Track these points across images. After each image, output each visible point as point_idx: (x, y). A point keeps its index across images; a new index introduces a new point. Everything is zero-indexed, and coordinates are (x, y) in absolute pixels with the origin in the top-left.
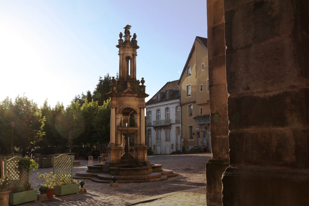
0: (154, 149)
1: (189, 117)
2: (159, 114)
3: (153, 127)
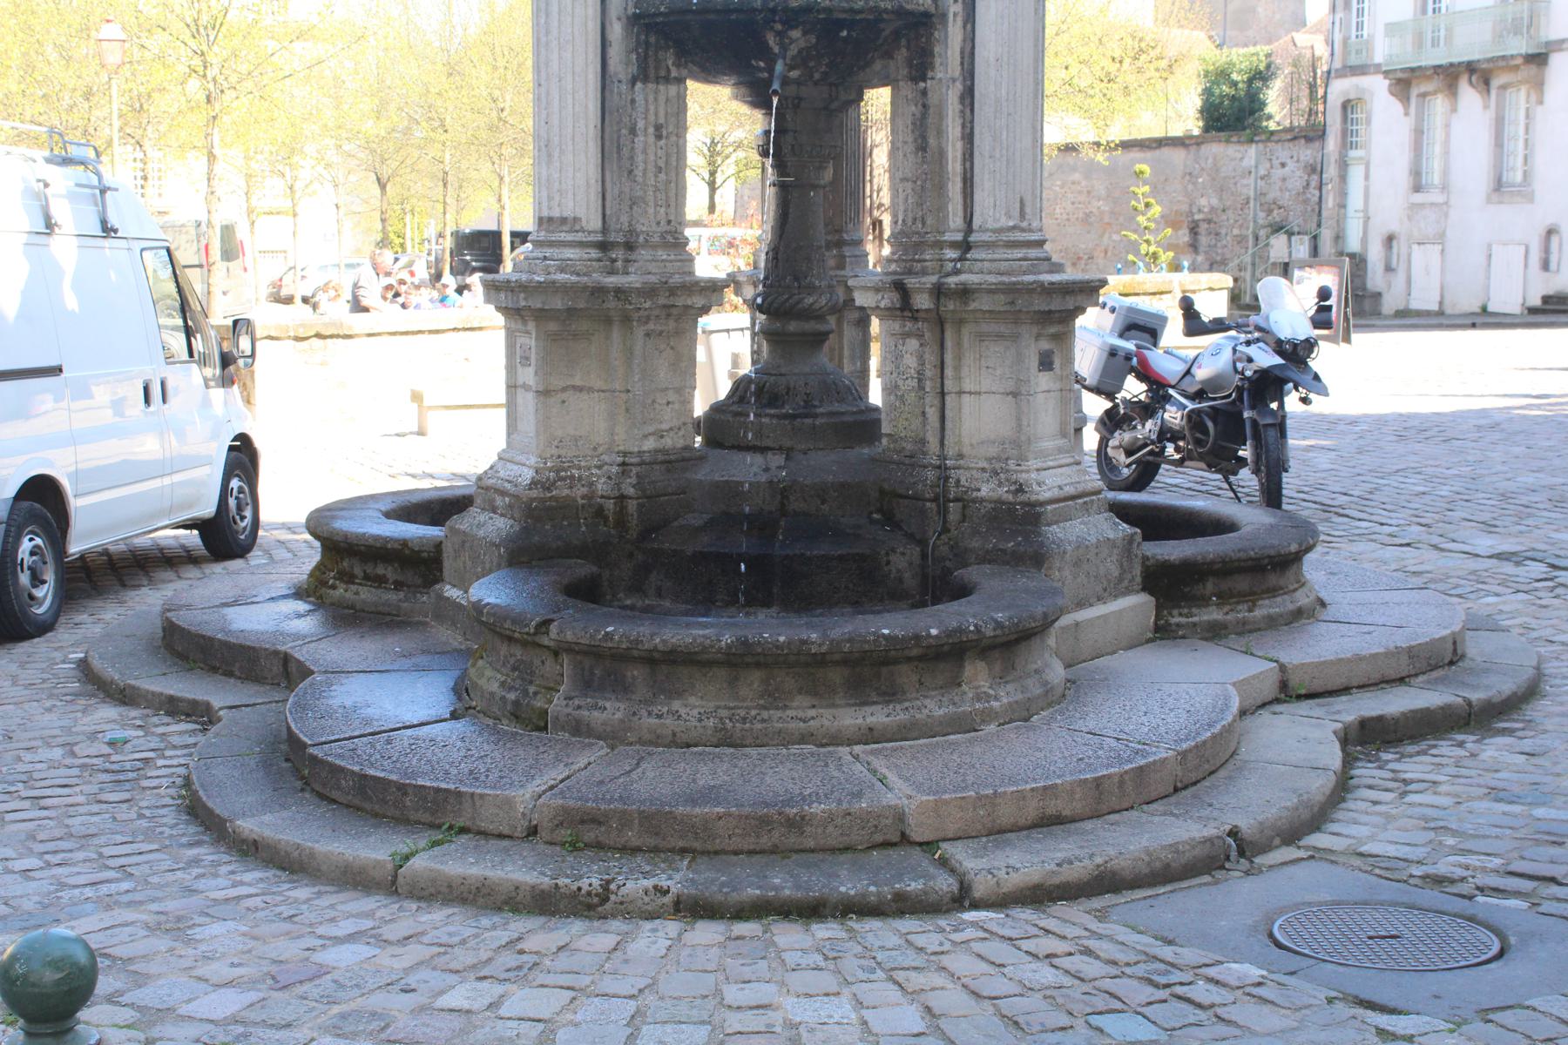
0: (1389, 269)
3: (1386, 73)
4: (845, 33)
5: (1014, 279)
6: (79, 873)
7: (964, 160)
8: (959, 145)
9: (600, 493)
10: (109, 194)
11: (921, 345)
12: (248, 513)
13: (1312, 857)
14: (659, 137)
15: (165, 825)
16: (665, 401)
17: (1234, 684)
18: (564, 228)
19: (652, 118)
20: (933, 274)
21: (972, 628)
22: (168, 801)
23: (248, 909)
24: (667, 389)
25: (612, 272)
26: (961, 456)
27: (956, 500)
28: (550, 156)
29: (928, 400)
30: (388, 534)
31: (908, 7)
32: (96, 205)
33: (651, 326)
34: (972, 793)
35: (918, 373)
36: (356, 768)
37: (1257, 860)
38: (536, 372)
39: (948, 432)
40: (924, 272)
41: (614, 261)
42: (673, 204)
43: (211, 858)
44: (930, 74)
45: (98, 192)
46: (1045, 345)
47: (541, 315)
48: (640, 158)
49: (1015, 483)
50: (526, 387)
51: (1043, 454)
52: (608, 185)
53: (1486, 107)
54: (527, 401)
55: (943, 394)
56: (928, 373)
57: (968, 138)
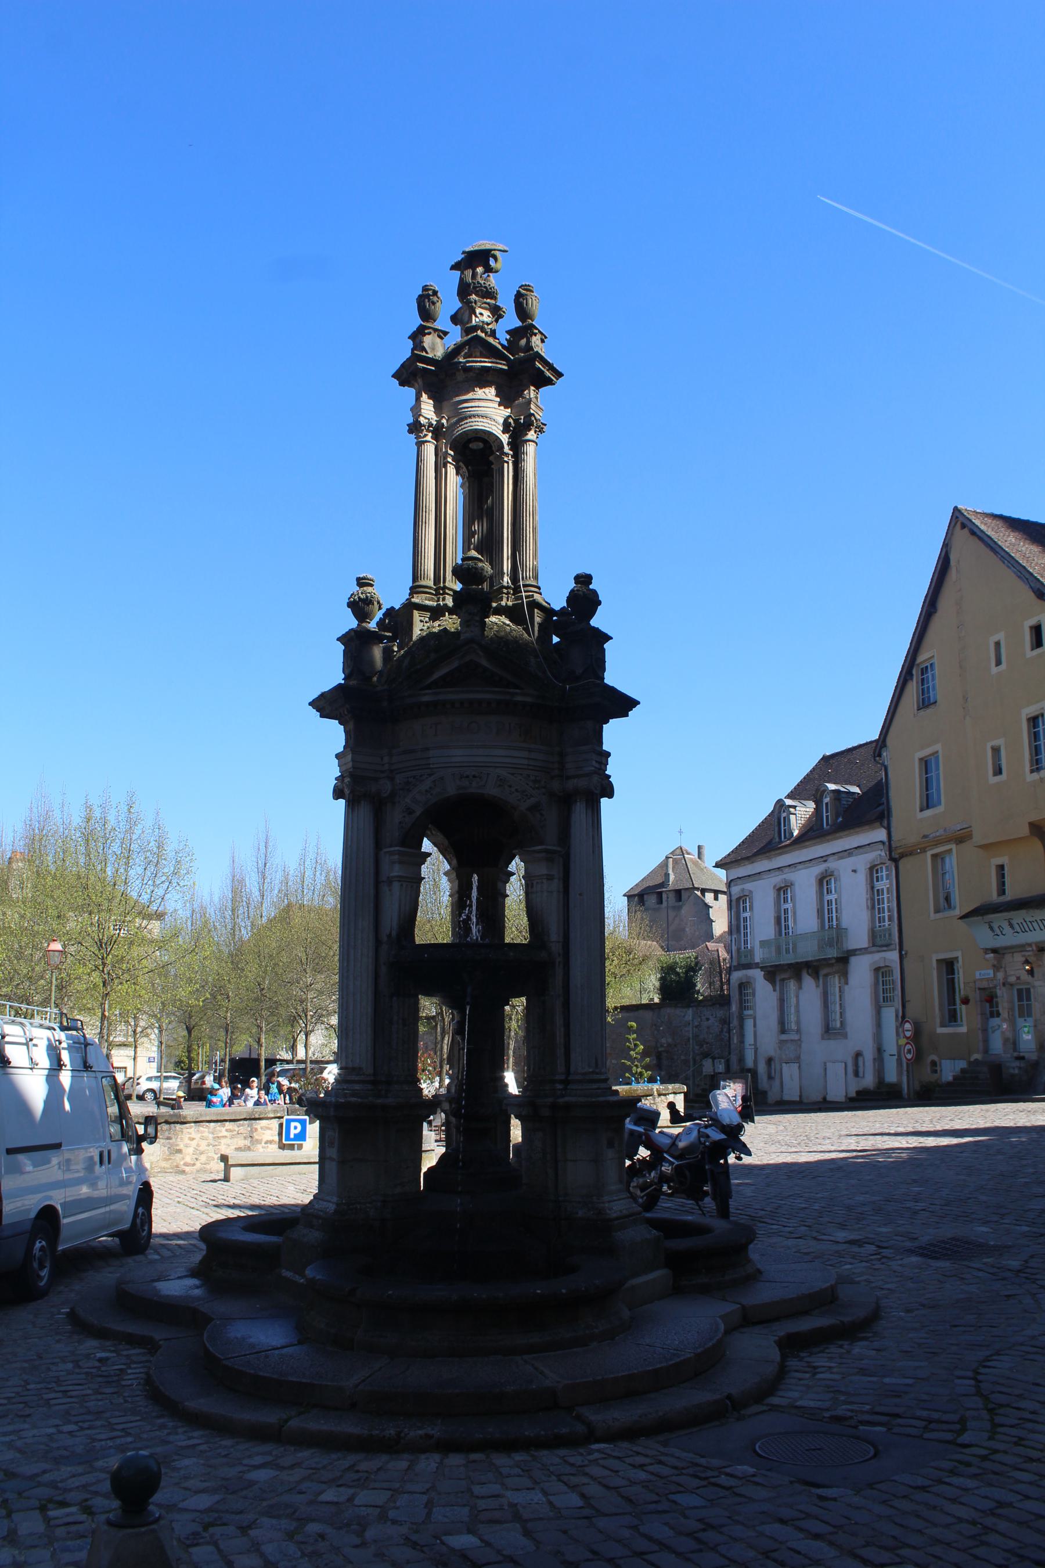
0: (770, 1077)
1: (939, 916)
2: (829, 897)
3: (762, 969)
5: (594, 1100)
6: (100, 1433)
8: (562, 1029)
10: (89, 1047)
12: (146, 1228)
13: (770, 1410)
15: (140, 1406)
17: (720, 1317)
21: (583, 1289)
22: (138, 1393)
23: (201, 1451)
30: (249, 1240)
32: (82, 1053)
34: (591, 1379)
36: (252, 1372)
37: (742, 1412)
43: (171, 1424)
45: (83, 1046)
50: (331, 1159)
53: (817, 986)
54: (332, 1167)
57: (567, 1025)
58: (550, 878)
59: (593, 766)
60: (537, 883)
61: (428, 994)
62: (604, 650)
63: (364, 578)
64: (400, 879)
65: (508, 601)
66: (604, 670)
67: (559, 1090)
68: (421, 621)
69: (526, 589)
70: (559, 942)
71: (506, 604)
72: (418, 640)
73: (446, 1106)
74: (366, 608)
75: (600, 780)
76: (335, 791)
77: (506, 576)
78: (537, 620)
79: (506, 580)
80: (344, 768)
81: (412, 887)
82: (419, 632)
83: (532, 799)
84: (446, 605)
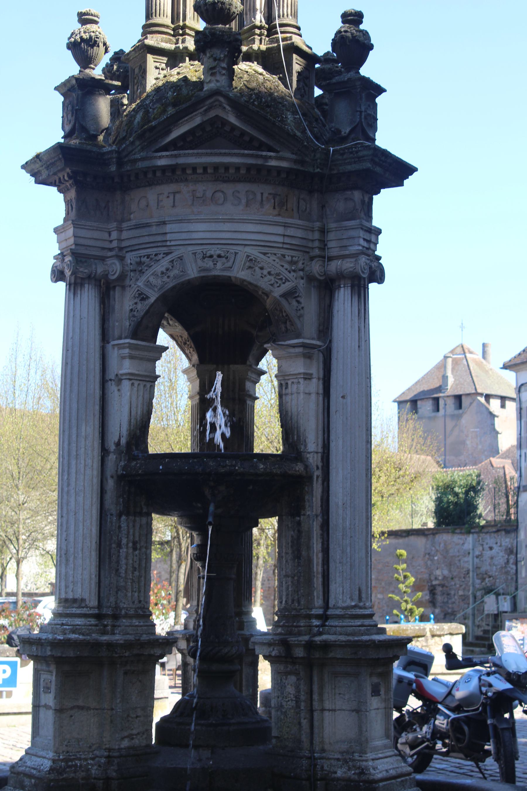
4: (251, 487)
5: (356, 638)
7: (323, 565)
8: (320, 555)
9: (93, 776)
11: (298, 679)
14: (135, 549)
16: (135, 716)
18: (75, 605)
19: (131, 538)
20: (305, 635)
24: (136, 708)
25: (104, 633)
26: (323, 750)
27: (321, 779)
28: (67, 560)
29: (303, 715)
31: (290, 472)
33: (128, 668)
35: (296, 697)
38: (55, 698)
39: (316, 736)
40: (300, 634)
41: (105, 626)
42: (142, 590)
44: (303, 512)
46: (375, 680)
47: (59, 661)
48: (123, 562)
49: (359, 768)
50: (47, 707)
51: (375, 749)
52: (102, 579)
55: (311, 711)
56: (303, 698)
57: (326, 550)
58: (308, 377)
59: (359, 245)
60: (293, 383)
61: (164, 511)
62: (376, 105)
63: (87, 14)
64: (131, 377)
65: (261, 43)
66: (375, 129)
67: (317, 626)
68: (157, 68)
69: (283, 29)
70: (317, 453)
71: (259, 48)
72: (152, 91)
73: (183, 644)
74: (90, 51)
75: (368, 262)
76: (53, 272)
77: (258, 12)
78: (297, 68)
79: (259, 19)
80: (64, 245)
81: (145, 386)
82: (154, 81)
83: (287, 283)
84: (186, 48)
